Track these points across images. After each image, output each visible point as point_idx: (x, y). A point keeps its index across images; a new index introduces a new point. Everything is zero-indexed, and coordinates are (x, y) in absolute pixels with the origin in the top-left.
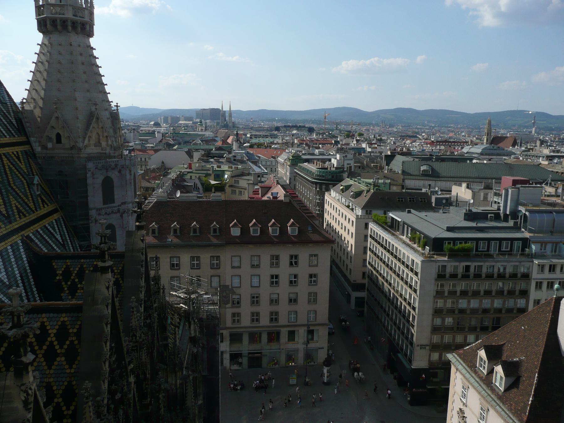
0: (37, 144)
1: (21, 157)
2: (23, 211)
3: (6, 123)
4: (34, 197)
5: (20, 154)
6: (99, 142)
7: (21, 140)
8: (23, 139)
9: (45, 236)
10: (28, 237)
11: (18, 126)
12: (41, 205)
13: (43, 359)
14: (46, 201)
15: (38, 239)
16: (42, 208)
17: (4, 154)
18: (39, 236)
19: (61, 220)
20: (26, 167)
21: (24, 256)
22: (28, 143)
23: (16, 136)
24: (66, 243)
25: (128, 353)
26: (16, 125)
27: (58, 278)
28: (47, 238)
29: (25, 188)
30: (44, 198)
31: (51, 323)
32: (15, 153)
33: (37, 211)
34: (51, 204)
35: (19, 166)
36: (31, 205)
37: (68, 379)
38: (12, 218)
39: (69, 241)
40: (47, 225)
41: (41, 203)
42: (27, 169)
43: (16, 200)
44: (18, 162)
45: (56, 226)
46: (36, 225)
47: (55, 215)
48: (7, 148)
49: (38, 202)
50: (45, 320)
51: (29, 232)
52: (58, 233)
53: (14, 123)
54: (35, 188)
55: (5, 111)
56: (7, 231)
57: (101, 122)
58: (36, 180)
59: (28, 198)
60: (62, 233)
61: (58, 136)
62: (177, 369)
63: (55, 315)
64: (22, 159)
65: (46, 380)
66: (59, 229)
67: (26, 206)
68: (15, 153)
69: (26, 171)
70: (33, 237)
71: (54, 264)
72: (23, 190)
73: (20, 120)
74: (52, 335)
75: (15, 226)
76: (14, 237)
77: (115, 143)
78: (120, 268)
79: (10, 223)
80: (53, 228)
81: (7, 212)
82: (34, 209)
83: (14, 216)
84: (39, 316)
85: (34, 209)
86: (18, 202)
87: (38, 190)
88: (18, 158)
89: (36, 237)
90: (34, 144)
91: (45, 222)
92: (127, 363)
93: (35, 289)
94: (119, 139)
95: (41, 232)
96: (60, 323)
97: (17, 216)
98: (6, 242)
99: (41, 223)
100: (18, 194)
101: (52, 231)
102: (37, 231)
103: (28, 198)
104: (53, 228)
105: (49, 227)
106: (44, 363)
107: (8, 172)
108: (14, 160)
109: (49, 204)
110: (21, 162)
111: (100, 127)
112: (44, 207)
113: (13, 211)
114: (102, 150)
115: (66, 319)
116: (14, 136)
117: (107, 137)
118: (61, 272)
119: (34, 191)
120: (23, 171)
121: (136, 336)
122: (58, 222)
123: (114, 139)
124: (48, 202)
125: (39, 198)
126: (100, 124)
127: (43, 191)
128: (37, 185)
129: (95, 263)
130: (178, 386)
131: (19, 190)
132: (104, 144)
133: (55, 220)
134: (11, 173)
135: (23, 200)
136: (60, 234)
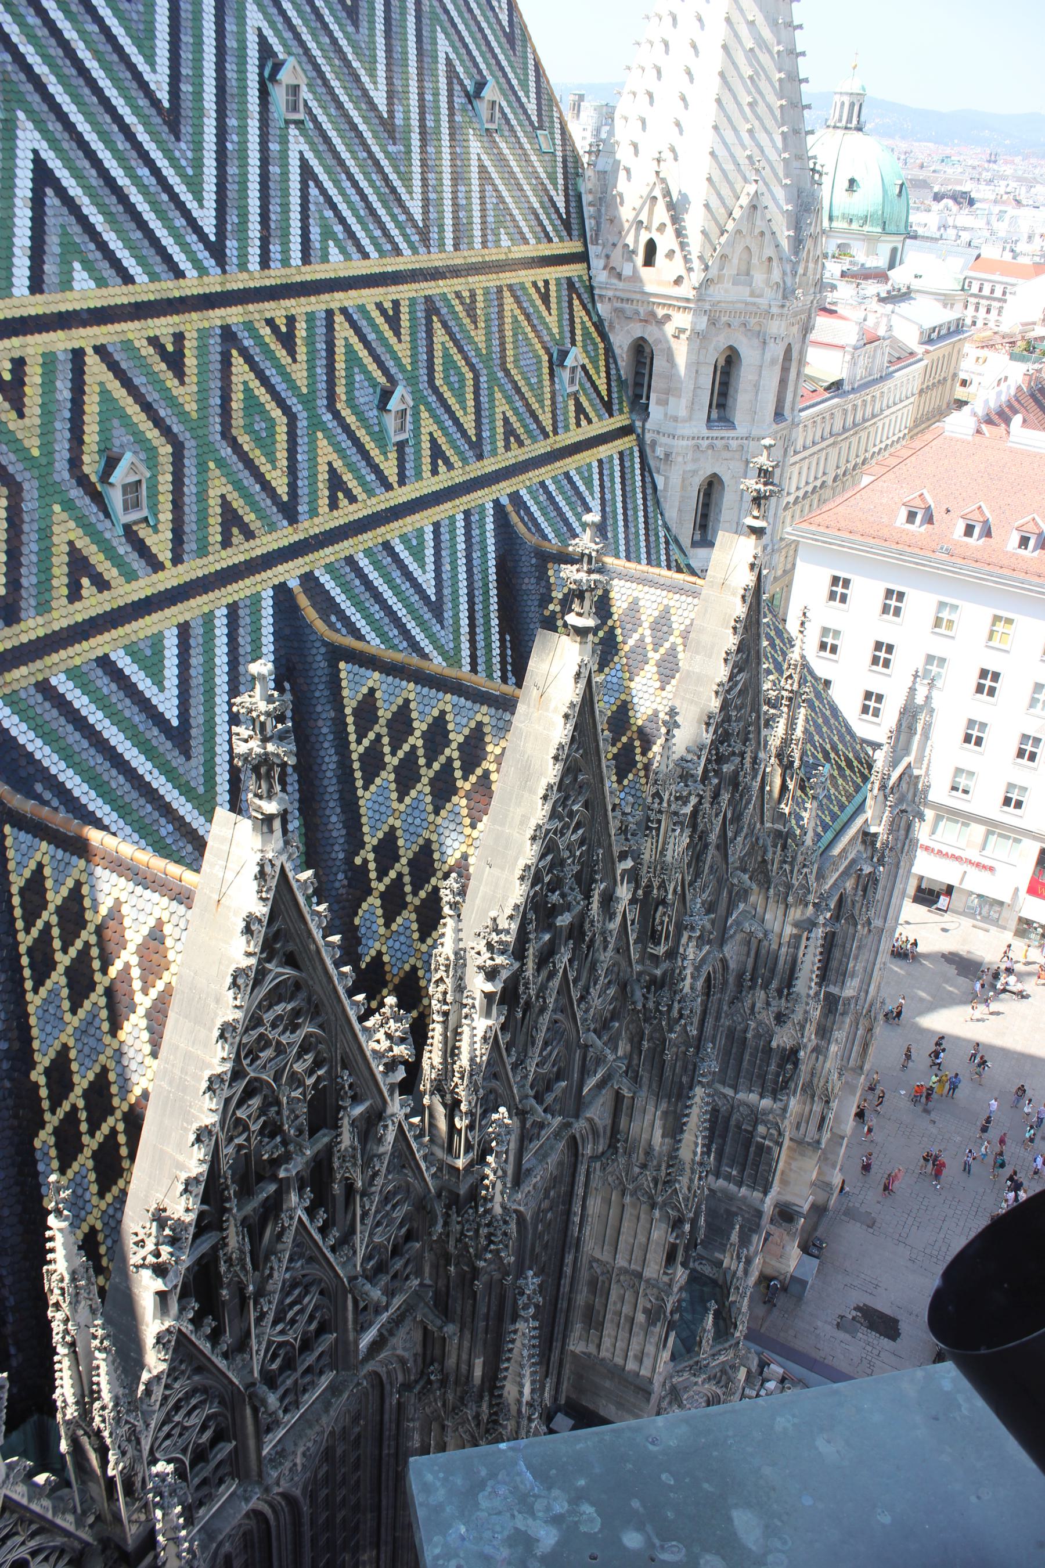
0: (601, 263)
1: (553, 294)
2: (520, 431)
3: (536, 205)
4: (559, 399)
5: (553, 288)
6: (748, 274)
7: (566, 251)
8: (573, 246)
9: (559, 499)
10: (515, 497)
11: (568, 212)
12: (572, 421)
13: (427, 789)
14: (589, 409)
15: (537, 503)
16: (573, 426)
17: (510, 287)
18: (543, 498)
19: (617, 462)
20: (560, 321)
21: (491, 541)
22: (583, 257)
23: (556, 239)
24: (610, 522)
25: (623, 830)
26: (563, 210)
27: (551, 607)
28: (562, 504)
29: (539, 376)
30: (586, 404)
31: (458, 719)
32: (541, 284)
33: (556, 433)
34: (600, 418)
35: (541, 317)
36: (546, 420)
37: (464, 848)
38: (487, 448)
39: (620, 517)
40: (572, 473)
41: (572, 414)
42: (560, 327)
43: (510, 401)
44: (542, 308)
45: (596, 476)
46: (543, 470)
47: (602, 448)
48: (523, 273)
49: (566, 413)
50: (448, 708)
51: (520, 484)
52: (597, 495)
53: (561, 205)
54: (566, 375)
55: (543, 175)
56: (467, 477)
57: (763, 216)
58: (576, 356)
59: (541, 402)
60: (608, 496)
61: (651, 248)
62: (790, 899)
63: (469, 704)
64: (553, 300)
65: (426, 834)
66: (602, 486)
67: (530, 421)
68: (541, 284)
69: (555, 331)
70: (526, 498)
71: (550, 573)
72: (534, 380)
73: (579, 197)
74: (454, 745)
75: (489, 465)
76: (480, 493)
77: (789, 280)
78: (688, 622)
79: (480, 457)
80: (589, 483)
81: (479, 435)
82: (549, 429)
83: (493, 443)
84: (441, 695)
85: (549, 429)
86: (515, 410)
87: (572, 381)
88: (545, 298)
89: (535, 498)
90: (594, 262)
91: (570, 464)
92: (616, 854)
93: (495, 622)
94: (811, 265)
95: (552, 488)
96: (473, 724)
97: (500, 444)
98: (457, 502)
99: (558, 464)
100: (518, 390)
101: (582, 488)
102: (542, 484)
103: (541, 402)
104: (589, 483)
105: (576, 478)
106: (429, 799)
107: (509, 333)
108: (532, 301)
109: (595, 419)
110: (549, 309)
111: (757, 231)
112: (578, 425)
113: (493, 429)
114: (752, 294)
115: (486, 720)
116: (550, 240)
117: (770, 259)
118: (560, 596)
119: (561, 382)
120: (549, 329)
121: (662, 800)
122: (606, 466)
123: (788, 268)
124: (592, 415)
125: (571, 402)
126: (758, 222)
127: (588, 385)
128: (573, 370)
129: (635, 594)
130: (785, 939)
131: (527, 379)
132: (759, 277)
133: (600, 462)
134: (515, 335)
135: (528, 405)
136: (603, 499)
